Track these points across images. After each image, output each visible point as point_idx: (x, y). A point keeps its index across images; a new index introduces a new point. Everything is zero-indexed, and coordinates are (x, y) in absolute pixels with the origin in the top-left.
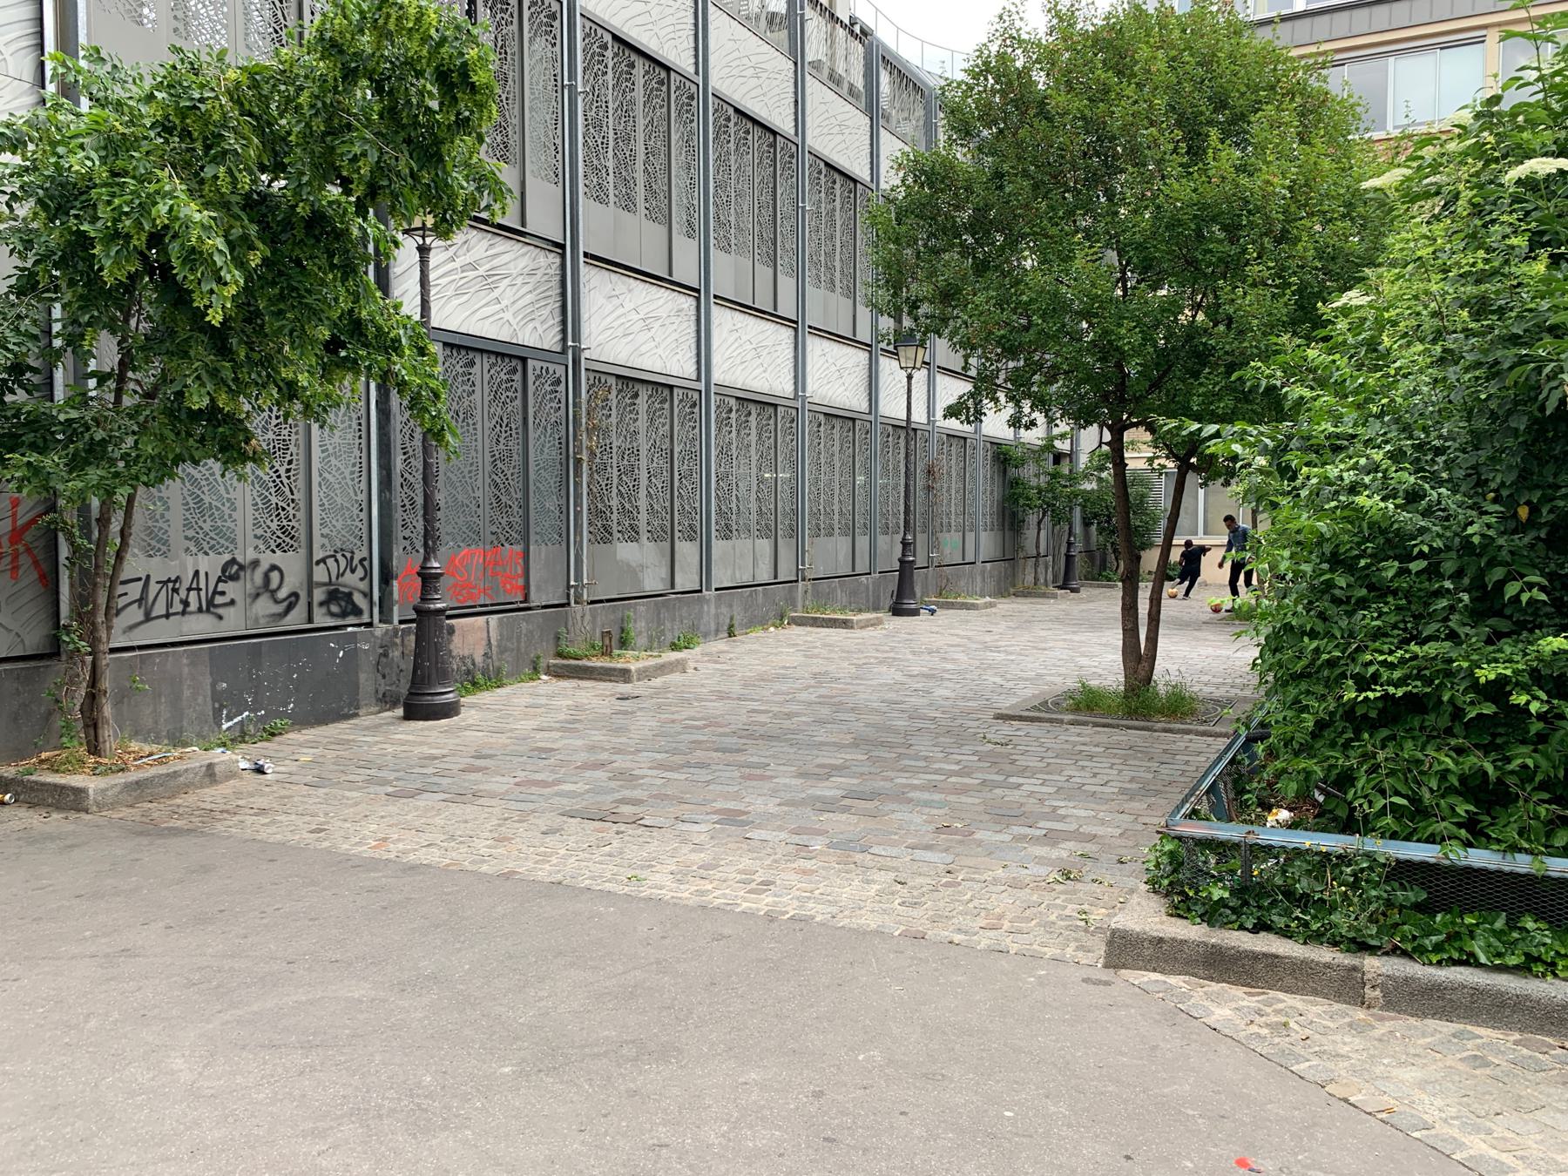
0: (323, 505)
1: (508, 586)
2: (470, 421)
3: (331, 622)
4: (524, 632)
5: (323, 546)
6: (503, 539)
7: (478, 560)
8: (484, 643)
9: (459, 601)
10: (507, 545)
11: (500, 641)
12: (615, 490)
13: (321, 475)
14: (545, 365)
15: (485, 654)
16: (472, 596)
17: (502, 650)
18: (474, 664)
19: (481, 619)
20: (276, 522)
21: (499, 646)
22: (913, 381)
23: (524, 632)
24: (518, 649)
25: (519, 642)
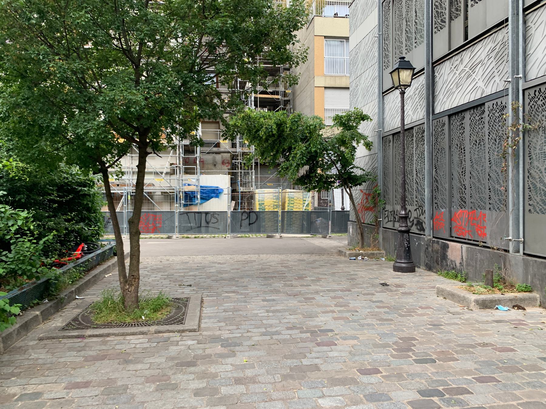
0: (530, 188)
1: (479, 232)
2: (463, 147)
3: (417, 232)
4: (479, 259)
5: (530, 210)
6: (477, 206)
7: (465, 216)
8: (460, 257)
9: (458, 234)
10: (479, 210)
11: (467, 259)
12: (415, 181)
13: (529, 172)
14: (495, 102)
15: (460, 263)
16: (463, 234)
17: (468, 265)
18: (456, 266)
19: (459, 245)
20: (539, 197)
21: (466, 261)
22: (405, 95)
23: (479, 259)
24: (476, 268)
25: (476, 263)
